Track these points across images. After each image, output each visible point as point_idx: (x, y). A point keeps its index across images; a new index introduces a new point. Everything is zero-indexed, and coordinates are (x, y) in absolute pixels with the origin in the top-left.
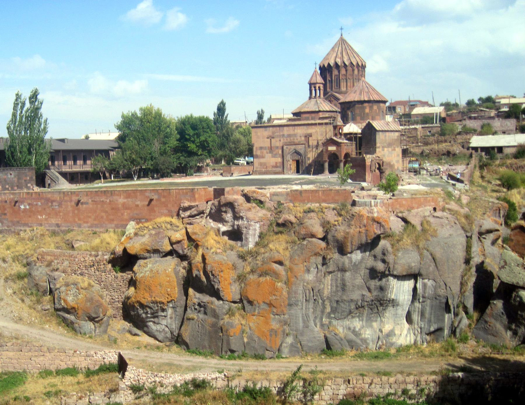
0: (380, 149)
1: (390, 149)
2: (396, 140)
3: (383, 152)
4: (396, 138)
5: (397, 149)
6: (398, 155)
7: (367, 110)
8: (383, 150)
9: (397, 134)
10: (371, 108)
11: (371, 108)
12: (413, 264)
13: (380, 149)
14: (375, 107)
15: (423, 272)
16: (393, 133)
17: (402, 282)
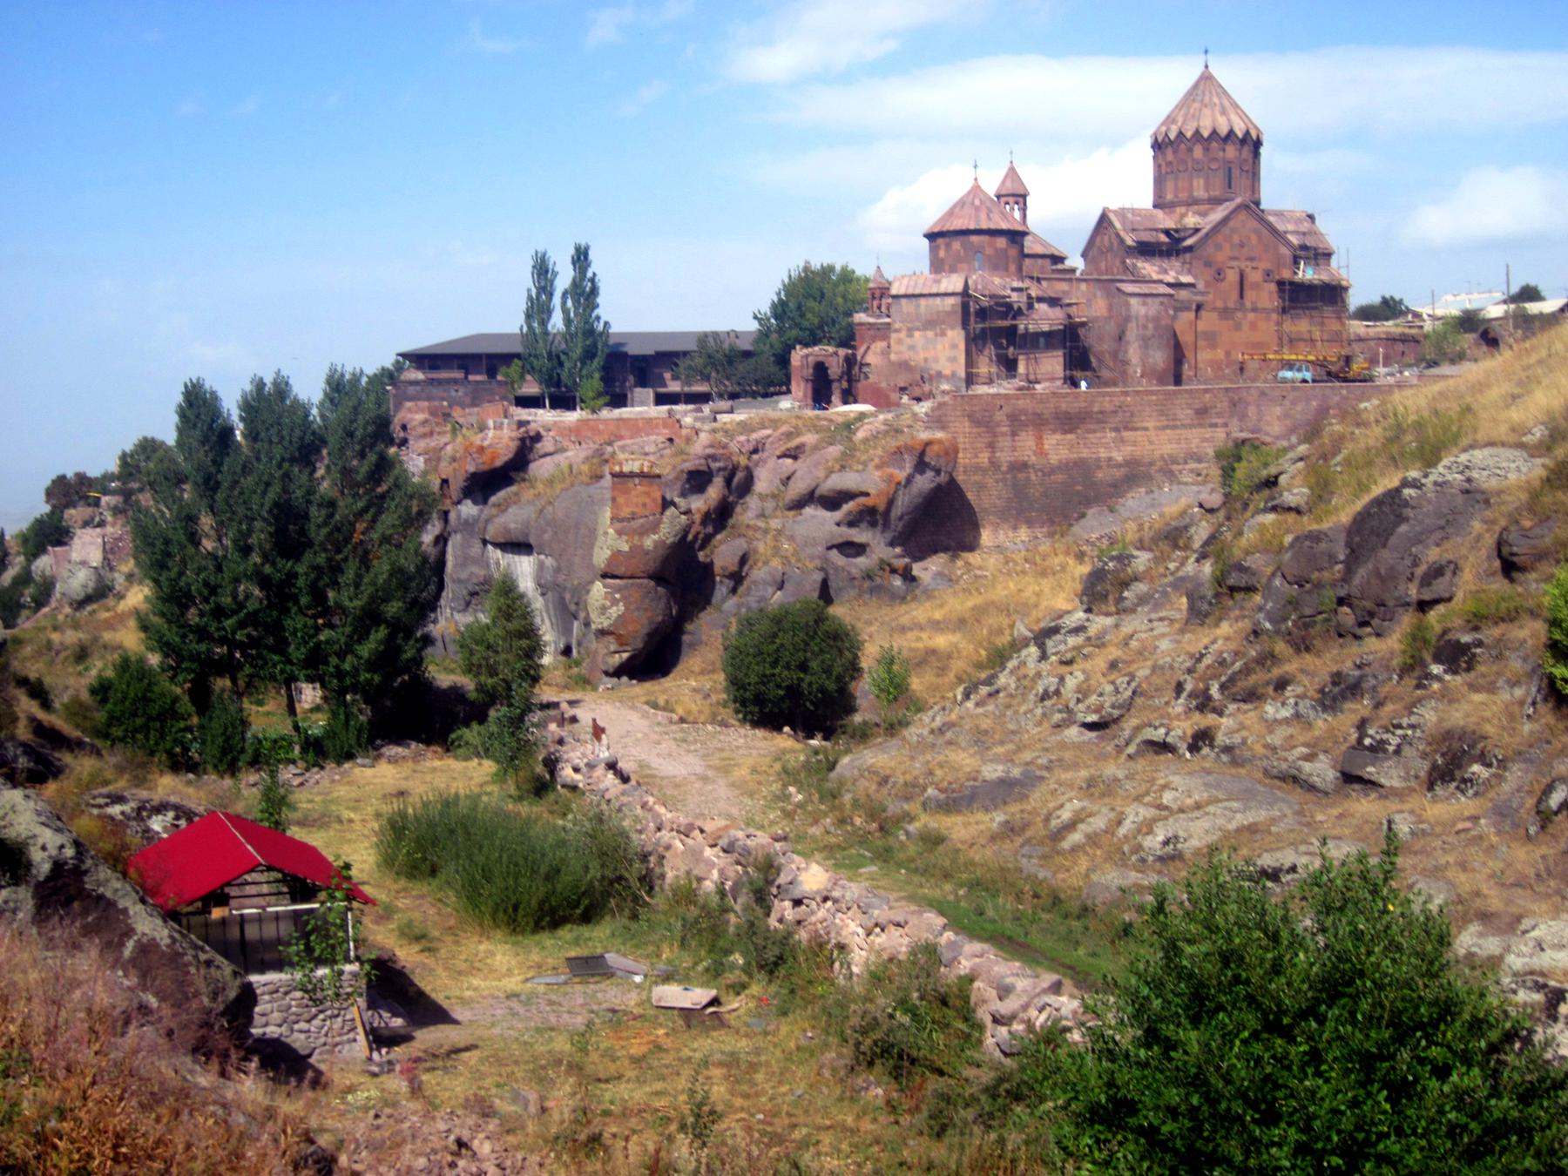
0: (903, 335)
1: (930, 334)
2: (949, 313)
3: (909, 341)
4: (948, 309)
5: (950, 333)
6: (954, 346)
7: (942, 253)
8: (910, 335)
9: (951, 301)
10: (948, 246)
11: (948, 246)
12: (512, 526)
13: (903, 335)
14: (956, 245)
15: (532, 541)
16: (938, 300)
17: (517, 558)
